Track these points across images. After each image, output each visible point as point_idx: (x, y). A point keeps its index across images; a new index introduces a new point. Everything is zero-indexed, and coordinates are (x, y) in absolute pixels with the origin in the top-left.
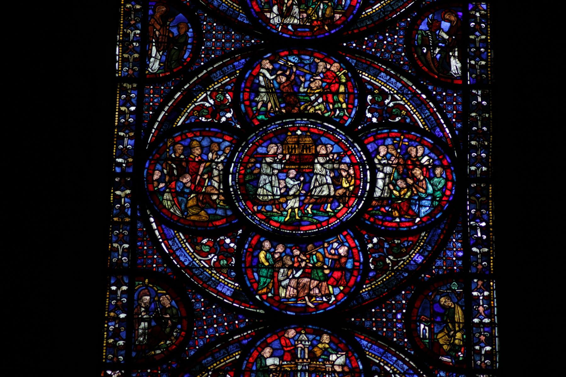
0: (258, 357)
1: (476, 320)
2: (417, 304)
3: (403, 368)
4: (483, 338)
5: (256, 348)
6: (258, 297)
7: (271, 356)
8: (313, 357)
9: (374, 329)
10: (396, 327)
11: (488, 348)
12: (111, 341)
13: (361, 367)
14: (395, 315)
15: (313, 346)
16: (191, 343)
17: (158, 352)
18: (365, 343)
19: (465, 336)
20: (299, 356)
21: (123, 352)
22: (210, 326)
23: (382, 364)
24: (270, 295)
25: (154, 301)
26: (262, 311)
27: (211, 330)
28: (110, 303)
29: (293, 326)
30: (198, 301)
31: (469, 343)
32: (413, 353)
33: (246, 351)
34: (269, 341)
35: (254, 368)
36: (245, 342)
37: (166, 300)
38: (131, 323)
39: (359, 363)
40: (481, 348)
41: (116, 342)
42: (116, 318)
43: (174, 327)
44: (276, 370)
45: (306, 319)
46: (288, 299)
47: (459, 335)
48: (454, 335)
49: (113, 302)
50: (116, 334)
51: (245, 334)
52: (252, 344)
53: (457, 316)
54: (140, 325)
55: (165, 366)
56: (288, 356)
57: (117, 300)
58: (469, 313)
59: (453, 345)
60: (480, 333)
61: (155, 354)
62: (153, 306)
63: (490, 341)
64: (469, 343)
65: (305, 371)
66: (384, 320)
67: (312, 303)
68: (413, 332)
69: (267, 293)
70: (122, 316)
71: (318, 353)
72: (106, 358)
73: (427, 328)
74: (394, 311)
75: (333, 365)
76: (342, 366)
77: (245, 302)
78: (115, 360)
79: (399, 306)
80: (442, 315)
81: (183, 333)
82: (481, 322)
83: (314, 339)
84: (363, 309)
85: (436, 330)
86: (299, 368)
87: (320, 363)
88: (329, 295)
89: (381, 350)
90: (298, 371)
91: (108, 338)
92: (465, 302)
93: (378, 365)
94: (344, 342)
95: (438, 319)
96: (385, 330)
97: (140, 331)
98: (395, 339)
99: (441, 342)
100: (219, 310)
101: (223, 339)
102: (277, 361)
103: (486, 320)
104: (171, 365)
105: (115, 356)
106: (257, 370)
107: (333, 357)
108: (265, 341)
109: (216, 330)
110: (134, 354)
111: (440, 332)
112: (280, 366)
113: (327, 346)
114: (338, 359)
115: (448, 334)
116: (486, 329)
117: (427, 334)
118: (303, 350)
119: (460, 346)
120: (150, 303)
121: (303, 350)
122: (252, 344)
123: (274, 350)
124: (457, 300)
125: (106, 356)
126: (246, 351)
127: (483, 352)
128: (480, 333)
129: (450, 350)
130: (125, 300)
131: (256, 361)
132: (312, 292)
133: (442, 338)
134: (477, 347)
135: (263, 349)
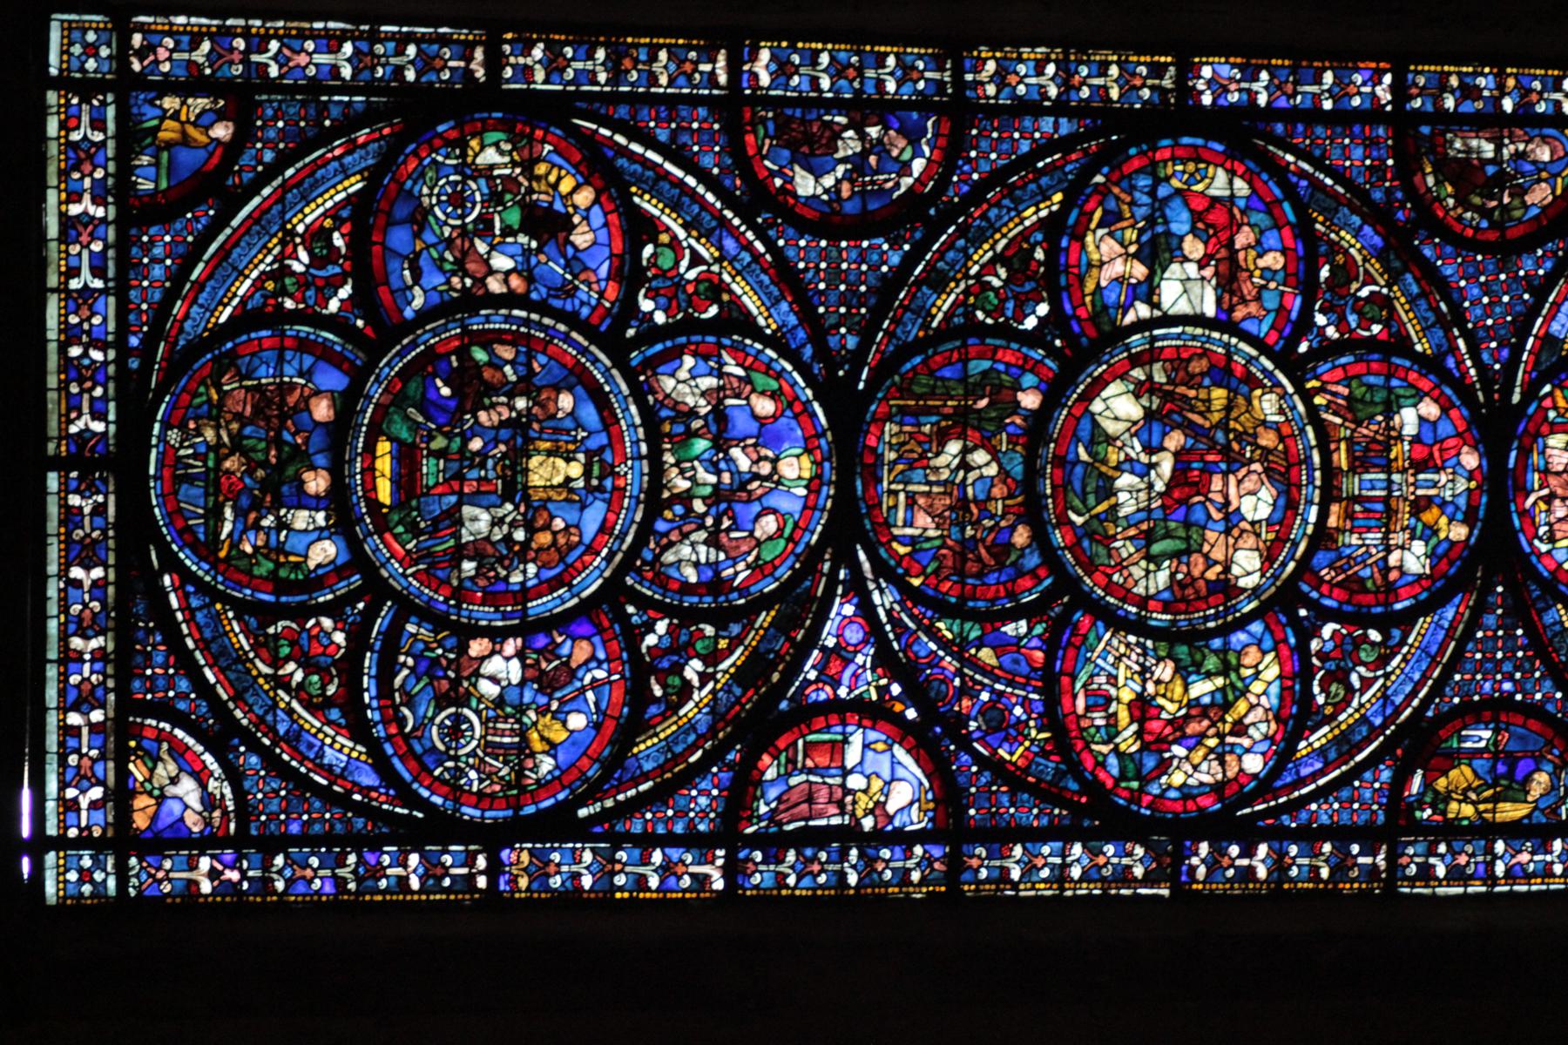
0: (1418, 390)
1: (1500, 846)
2: (1533, 724)
3: (1396, 693)
4: (1463, 860)
5: (1437, 386)
6: (1547, 388)
7: (1421, 419)
8: (1419, 506)
9: (1480, 634)
10: (1485, 679)
11: (1441, 871)
12: (1454, 81)
13: (1398, 606)
14: (1509, 677)
15: (1443, 504)
16: (1449, 249)
17: (1430, 181)
18: (1450, 613)
19: (1465, 823)
20: (1421, 476)
21: (1429, 108)
22: (1486, 289)
23: (1405, 650)
24: (1552, 414)
25: (1540, 171)
26: (1516, 398)
27: (1476, 291)
28: (1535, 77)
29: (1484, 463)
30: (1539, 263)
31: (1451, 831)
32: (1430, 714)
33: (1431, 364)
34: (1454, 413)
35: (1395, 382)
36: (1451, 363)
37: (1540, 195)
38: (1492, 122)
39: (1407, 603)
40: (1442, 856)
41: (1452, 92)
42: (1502, 91)
43: (1484, 212)
44: (1389, 428)
45: (1500, 490)
46: (1543, 452)
47: (1468, 810)
48: (1466, 800)
49: (1537, 85)
50: (1468, 91)
51: (1469, 363)
52: (1445, 376)
53: (1507, 806)
54: (1487, 140)
55: (1399, 195)
56: (1421, 453)
57: (1540, 93)
58: (1515, 832)
59: (1447, 798)
60: (1473, 855)
61: (1424, 175)
62: (1528, 167)
63: (1457, 875)
64: (1451, 831)
65: (1389, 488)
66: (1499, 655)
67: (1535, 503)
68: (1472, 713)
69: (1555, 408)
70: (1508, 105)
71: (1428, 516)
72: (1417, 73)
73: (1482, 744)
74: (1518, 675)
75: (1402, 548)
76: (1400, 568)
77: (1537, 363)
78: (1414, 91)
79: (1529, 686)
80: (1510, 775)
81: (1470, 232)
82: (1495, 857)
83: (1457, 508)
84: (1521, 611)
85: (1477, 763)
86: (1396, 477)
87: (1406, 519)
88: (1552, 539)
89: (1434, 649)
90: (1390, 473)
91: (1459, 74)
92: (1539, 825)
93: (1403, 642)
94: (1452, 571)
95: (1501, 769)
96: (1478, 656)
97: (1474, 143)
98: (1457, 677)
99: (1453, 773)
100: (1518, 308)
101: (1458, 316)
102: (1410, 429)
103: (1500, 869)
104: (1403, 207)
105: (1423, 92)
106: (1390, 390)
107: (1419, 547)
108: (1453, 406)
109: (1476, 302)
110: (1425, 130)
111: (1474, 771)
112: (1400, 438)
113: (1442, 535)
114: (1414, 559)
115: (1469, 788)
116: (1481, 868)
117: (1468, 745)
118: (1435, 484)
119: (1444, 813)
120: (1535, 162)
121: (1435, 484)
122: (1445, 376)
123: (1434, 424)
124: (1542, 805)
125: (1421, 73)
126: (1431, 364)
127: (1432, 860)
128: (1473, 855)
129: (1436, 792)
130: (1541, 108)
131: (1411, 386)
132: (1557, 502)
133: (1461, 775)
134: (1442, 848)
135: (1436, 401)
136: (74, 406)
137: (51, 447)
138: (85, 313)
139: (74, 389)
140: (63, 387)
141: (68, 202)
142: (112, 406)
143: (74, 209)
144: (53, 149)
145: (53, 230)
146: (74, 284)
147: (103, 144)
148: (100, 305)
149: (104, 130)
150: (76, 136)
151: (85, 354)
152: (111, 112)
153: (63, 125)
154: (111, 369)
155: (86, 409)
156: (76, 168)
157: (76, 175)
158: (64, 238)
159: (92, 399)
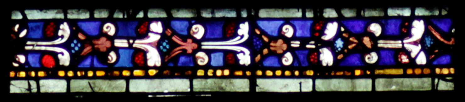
136: (391, 59)
137: (443, 86)
138: (280, 45)
139: (373, 58)
140: (370, 72)
141: (146, 68)
142: (392, 12)
143: (154, 58)
144: (80, 86)
145: (180, 85)
146: (245, 59)
147: (73, 23)
148: (270, 28)
149: (57, 23)
150: (65, 59)
151: (330, 44)
152: (34, 15)
153: (52, 75)
154: (348, 14)
155: (397, 44)
156: (103, 56)
157: (113, 57)
158: (189, 71)
159: (385, 36)
